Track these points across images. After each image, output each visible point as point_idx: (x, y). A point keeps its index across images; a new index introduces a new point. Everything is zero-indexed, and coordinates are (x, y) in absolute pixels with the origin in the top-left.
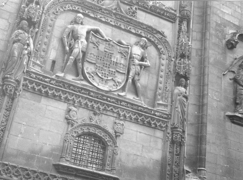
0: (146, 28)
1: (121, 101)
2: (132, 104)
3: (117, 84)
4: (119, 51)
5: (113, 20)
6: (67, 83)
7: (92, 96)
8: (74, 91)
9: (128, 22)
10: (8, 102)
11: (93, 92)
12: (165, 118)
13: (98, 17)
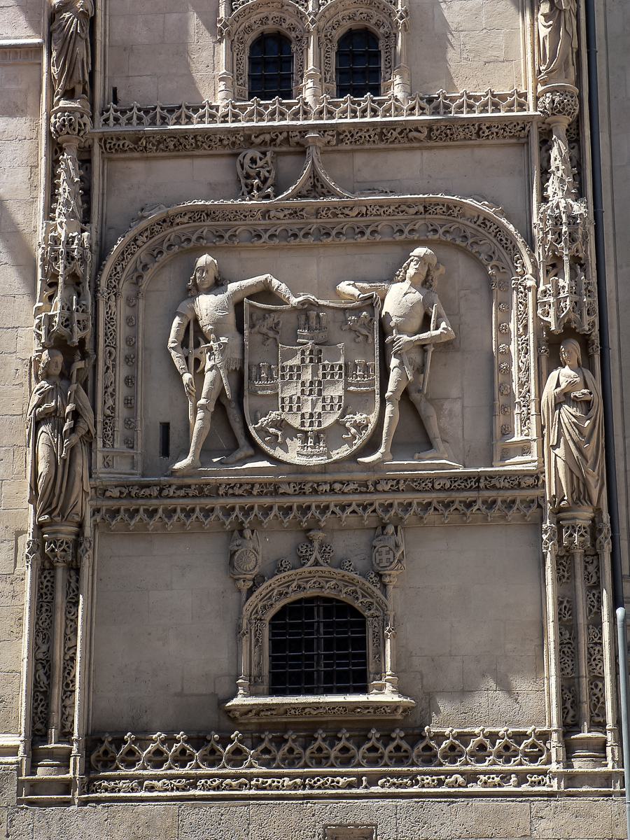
8: (233, 495)
10: (68, 580)
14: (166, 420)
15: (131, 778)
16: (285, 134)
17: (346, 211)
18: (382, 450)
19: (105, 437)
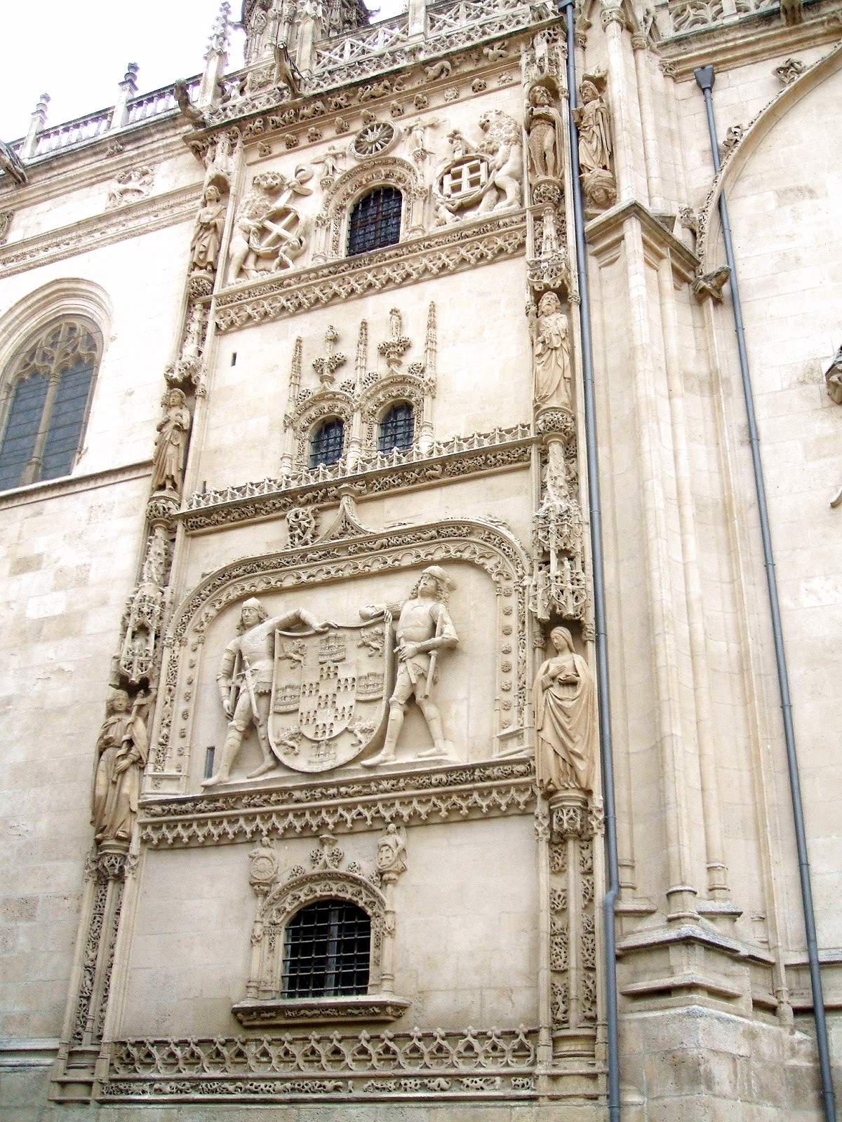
0: (438, 532)
1: (378, 780)
2: (411, 776)
3: (360, 736)
4: (360, 643)
5: (342, 565)
6: (232, 795)
7: (297, 801)
8: (255, 806)
9: (382, 546)
11: (301, 788)
12: (523, 774)
13: (304, 578)
14: (210, 745)
15: (145, 1080)
16: (324, 490)
17: (370, 545)
18: (383, 752)
19: (157, 762)
